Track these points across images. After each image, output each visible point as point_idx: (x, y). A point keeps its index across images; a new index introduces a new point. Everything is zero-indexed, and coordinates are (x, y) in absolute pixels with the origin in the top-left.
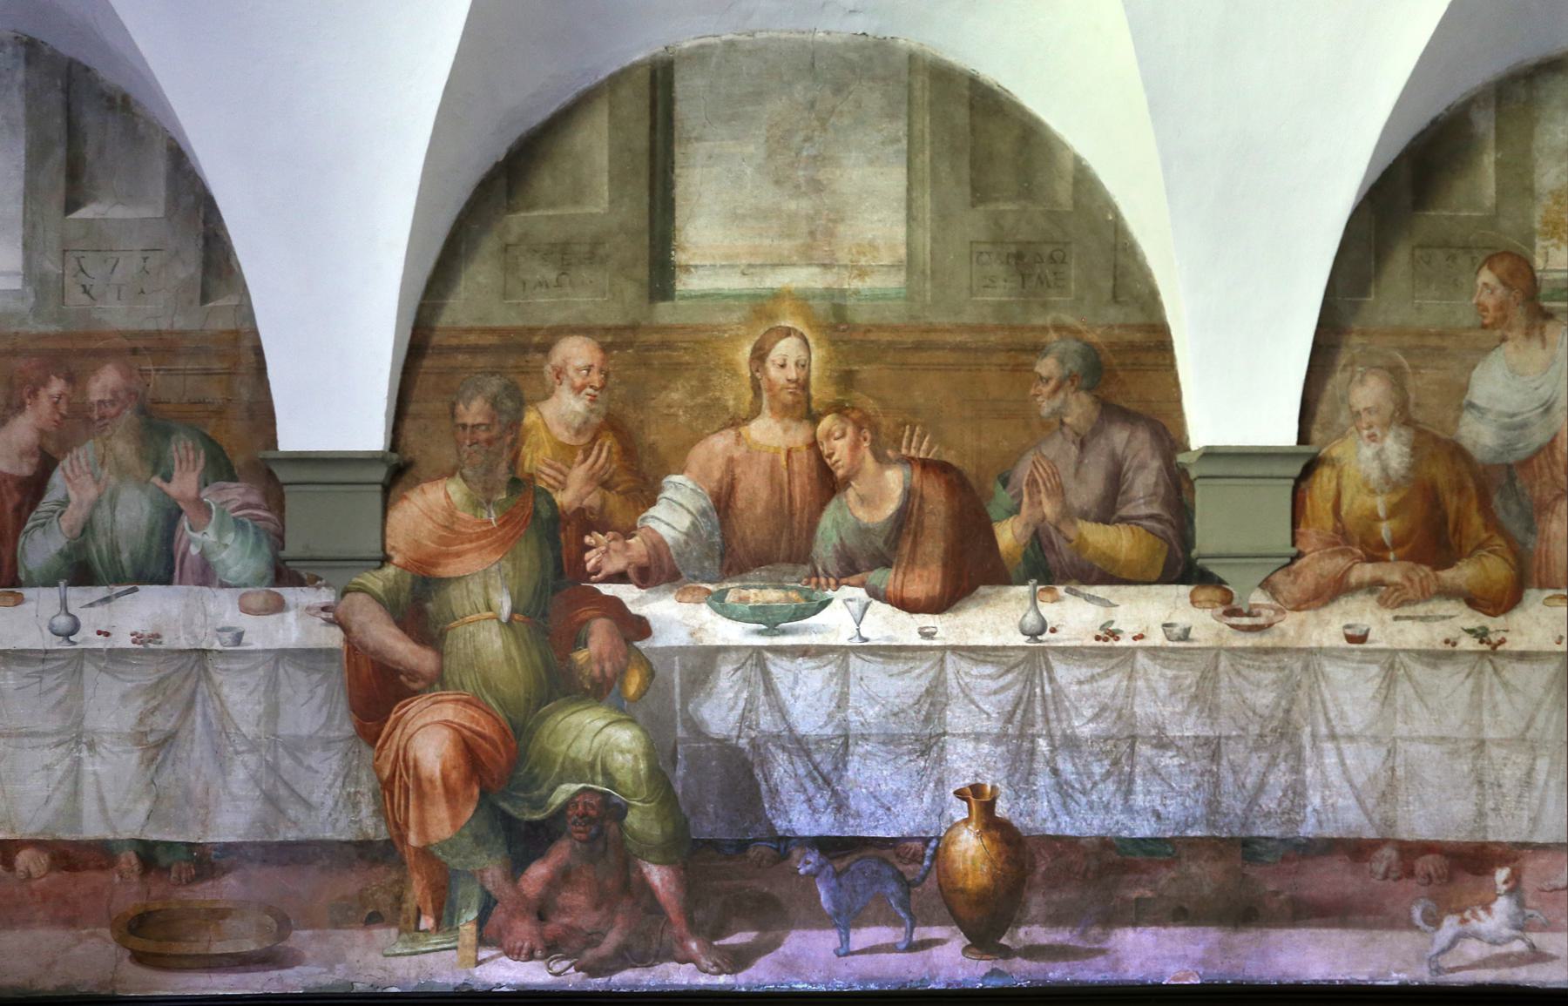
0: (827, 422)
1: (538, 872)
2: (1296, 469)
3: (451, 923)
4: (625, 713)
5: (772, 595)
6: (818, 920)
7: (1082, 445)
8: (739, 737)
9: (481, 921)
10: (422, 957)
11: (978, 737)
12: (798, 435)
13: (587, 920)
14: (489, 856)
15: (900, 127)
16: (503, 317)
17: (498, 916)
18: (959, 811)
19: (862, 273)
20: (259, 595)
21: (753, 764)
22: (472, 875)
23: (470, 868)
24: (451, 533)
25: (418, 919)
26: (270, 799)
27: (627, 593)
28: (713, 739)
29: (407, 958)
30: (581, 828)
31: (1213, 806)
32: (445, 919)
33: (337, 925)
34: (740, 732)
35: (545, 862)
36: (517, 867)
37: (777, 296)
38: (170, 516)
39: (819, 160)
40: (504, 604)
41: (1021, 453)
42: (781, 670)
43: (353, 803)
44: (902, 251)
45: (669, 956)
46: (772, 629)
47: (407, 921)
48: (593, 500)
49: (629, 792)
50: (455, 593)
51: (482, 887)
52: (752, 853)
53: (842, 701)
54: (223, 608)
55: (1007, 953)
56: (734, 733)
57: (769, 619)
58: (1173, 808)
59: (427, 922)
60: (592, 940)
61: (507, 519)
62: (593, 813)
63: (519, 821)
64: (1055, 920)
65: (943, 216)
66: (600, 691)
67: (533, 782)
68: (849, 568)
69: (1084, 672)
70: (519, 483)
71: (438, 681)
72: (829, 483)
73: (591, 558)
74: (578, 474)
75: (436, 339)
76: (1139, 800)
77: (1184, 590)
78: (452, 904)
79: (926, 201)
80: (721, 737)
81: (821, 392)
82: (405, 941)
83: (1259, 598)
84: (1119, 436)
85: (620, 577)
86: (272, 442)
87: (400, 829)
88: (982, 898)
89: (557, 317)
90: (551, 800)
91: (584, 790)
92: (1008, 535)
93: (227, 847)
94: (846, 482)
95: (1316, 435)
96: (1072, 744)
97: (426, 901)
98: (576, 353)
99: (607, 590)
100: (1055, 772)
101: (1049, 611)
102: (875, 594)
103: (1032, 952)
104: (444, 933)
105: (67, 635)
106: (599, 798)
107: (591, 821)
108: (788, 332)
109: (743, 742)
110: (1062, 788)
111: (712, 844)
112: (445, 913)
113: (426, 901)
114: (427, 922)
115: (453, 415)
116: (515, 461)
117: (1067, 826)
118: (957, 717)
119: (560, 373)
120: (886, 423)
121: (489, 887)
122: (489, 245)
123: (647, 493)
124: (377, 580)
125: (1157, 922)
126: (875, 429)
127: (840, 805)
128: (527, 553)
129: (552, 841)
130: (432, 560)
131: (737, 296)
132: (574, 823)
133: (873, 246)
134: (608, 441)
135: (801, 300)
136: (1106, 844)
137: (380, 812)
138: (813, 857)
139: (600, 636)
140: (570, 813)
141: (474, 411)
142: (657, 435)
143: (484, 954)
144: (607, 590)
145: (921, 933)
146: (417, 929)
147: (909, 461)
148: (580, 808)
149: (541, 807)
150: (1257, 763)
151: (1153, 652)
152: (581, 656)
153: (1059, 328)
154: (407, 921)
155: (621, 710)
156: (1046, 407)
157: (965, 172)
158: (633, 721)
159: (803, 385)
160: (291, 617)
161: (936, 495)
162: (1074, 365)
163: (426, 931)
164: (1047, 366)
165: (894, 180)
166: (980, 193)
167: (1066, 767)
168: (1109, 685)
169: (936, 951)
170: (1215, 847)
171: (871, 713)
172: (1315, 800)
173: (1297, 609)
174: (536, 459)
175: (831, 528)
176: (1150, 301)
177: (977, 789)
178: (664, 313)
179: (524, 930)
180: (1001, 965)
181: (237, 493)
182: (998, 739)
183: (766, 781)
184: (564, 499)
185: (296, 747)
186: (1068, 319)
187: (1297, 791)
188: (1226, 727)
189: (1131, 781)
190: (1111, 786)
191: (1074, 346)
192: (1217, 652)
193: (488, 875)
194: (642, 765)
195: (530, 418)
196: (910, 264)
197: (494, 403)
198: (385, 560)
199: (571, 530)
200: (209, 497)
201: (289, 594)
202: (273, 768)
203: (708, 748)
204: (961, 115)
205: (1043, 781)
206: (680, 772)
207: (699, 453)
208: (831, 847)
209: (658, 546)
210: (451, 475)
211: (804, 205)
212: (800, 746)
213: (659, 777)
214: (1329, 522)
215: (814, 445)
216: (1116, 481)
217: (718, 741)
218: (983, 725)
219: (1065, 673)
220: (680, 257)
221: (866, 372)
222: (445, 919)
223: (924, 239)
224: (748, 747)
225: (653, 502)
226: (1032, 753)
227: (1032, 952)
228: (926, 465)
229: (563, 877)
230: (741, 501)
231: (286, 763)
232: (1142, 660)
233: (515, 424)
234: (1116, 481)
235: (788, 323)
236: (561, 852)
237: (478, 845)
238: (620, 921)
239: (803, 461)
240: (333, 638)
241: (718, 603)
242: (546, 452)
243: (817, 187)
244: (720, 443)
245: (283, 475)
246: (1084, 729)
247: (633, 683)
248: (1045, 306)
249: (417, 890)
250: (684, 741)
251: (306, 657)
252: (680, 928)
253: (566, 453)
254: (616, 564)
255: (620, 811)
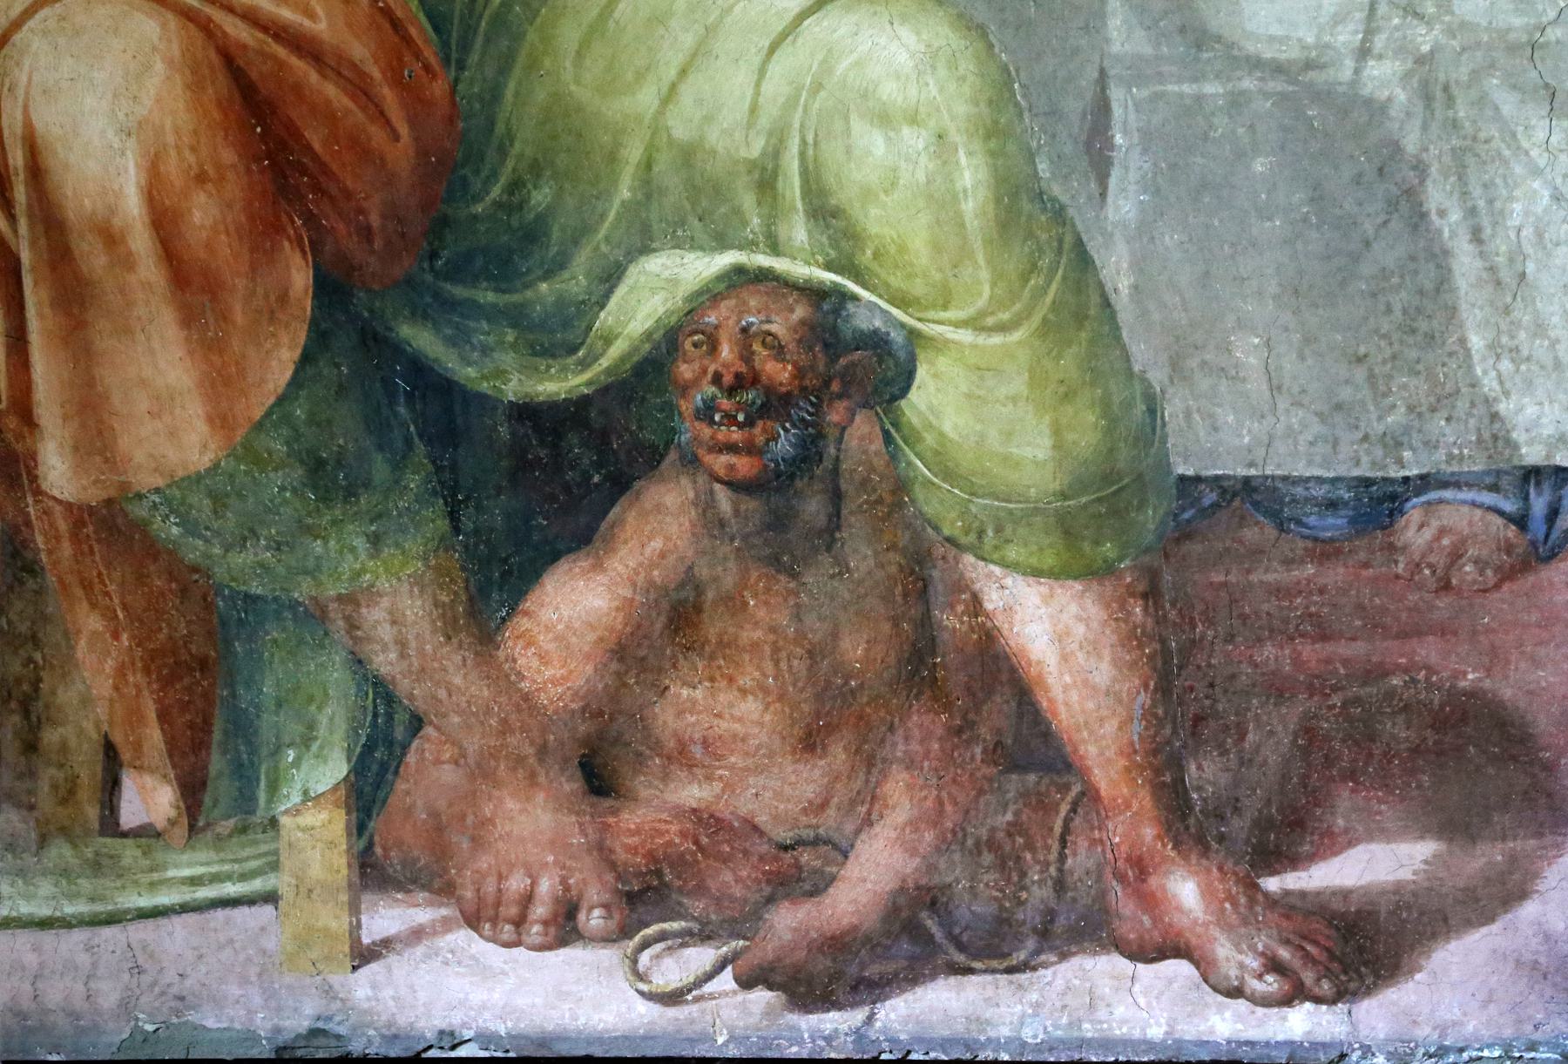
3: (245, 802)
8: (1364, 52)
10: (139, 932)
14: (375, 541)
21: (1421, 168)
22: (314, 616)
23: (303, 590)
25: (112, 786)
28: (1256, 64)
29: (79, 935)
30: (736, 435)
34: (1369, 32)
35: (598, 567)
47: (67, 794)
49: (918, 288)
51: (358, 662)
56: (1347, 37)
62: (779, 373)
63: (484, 402)
78: (243, 727)
80: (1291, 53)
82: (65, 873)
90: (606, 318)
91: (740, 278)
97: (134, 717)
104: (219, 842)
106: (800, 312)
107: (775, 405)
112: (217, 763)
113: (134, 717)
121: (385, 662)
129: (620, 485)
132: (706, 413)
140: (686, 371)
146: (110, 825)
148: (726, 352)
149: (573, 350)
154: (67, 794)
163: (148, 833)
183: (1477, 236)
193: (375, 615)
203: (1237, 101)
206: (1124, 205)
217: (1278, 69)
222: (221, 787)
224: (1401, 96)
237: (325, 498)
250: (1140, 72)
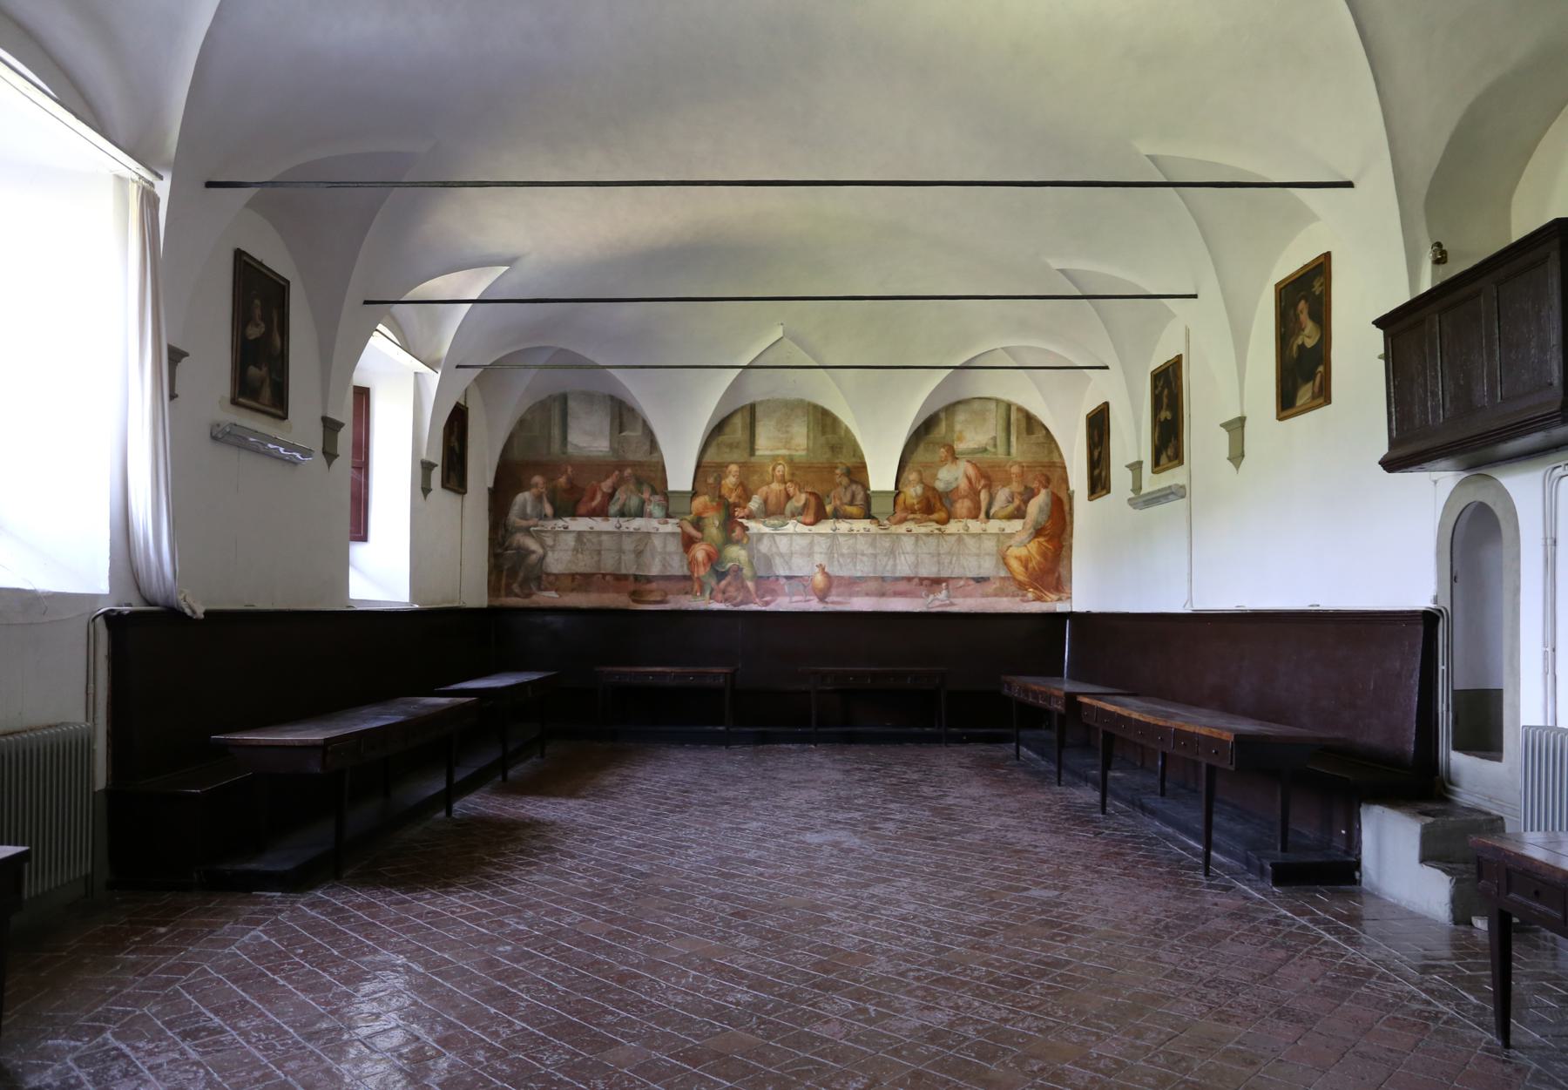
0: (789, 484)
1: (723, 583)
2: (894, 495)
4: (743, 547)
5: (776, 522)
6: (785, 595)
7: (846, 488)
9: (711, 593)
11: (821, 553)
12: (782, 487)
13: (735, 594)
15: (806, 419)
16: (718, 460)
17: (714, 593)
18: (817, 570)
19: (797, 451)
20: (662, 520)
24: (706, 508)
26: (664, 565)
27: (744, 521)
31: (875, 570)
32: (702, 592)
33: (678, 594)
36: (719, 581)
37: (778, 456)
38: (643, 502)
39: (788, 426)
40: (717, 523)
41: (831, 490)
42: (777, 538)
43: (682, 566)
44: (806, 446)
45: (752, 602)
46: (776, 530)
48: (737, 501)
50: (706, 520)
52: (771, 579)
53: (791, 545)
54: (654, 523)
55: (827, 603)
57: (775, 527)
58: (866, 569)
59: (698, 594)
60: (735, 599)
61: (719, 504)
64: (838, 595)
65: (815, 438)
66: (737, 542)
67: (722, 563)
68: (793, 516)
69: (846, 539)
70: (721, 496)
71: (702, 540)
72: (789, 497)
73: (736, 513)
74: (734, 495)
75: (703, 464)
76: (858, 568)
77: (869, 520)
79: (811, 436)
81: (787, 477)
83: (886, 522)
84: (854, 487)
85: (743, 518)
86: (666, 487)
87: (693, 572)
88: (821, 590)
89: (729, 460)
92: (829, 508)
93: (654, 576)
94: (792, 497)
95: (900, 486)
96: (842, 555)
98: (734, 468)
99: (740, 520)
100: (839, 561)
101: (838, 525)
102: (798, 521)
103: (833, 603)
105: (619, 528)
108: (780, 464)
109: (769, 555)
110: (840, 565)
111: (761, 577)
114: (698, 594)
115: (706, 481)
116: (720, 491)
117: (841, 574)
118: (817, 549)
119: (730, 472)
120: (802, 484)
122: (714, 443)
123: (749, 499)
124: (689, 518)
125: (862, 596)
126: (800, 486)
127: (790, 569)
128: (723, 512)
130: (701, 513)
131: (769, 456)
133: (799, 445)
134: (741, 488)
135: (783, 457)
136: (850, 578)
137: (689, 569)
138: (784, 580)
139: (738, 530)
141: (711, 480)
142: (751, 487)
143: (711, 601)
144: (740, 520)
145: (808, 598)
147: (807, 492)
150: (885, 559)
151: (862, 534)
152: (734, 535)
153: (841, 463)
155: (742, 546)
156: (838, 480)
157: (820, 428)
158: (744, 549)
159: (783, 476)
160: (669, 525)
161: (813, 500)
162: (844, 471)
164: (838, 471)
165: (804, 430)
166: (824, 432)
167: (841, 560)
168: (851, 541)
169: (812, 602)
170: (876, 578)
171: (797, 548)
172: (899, 568)
173: (895, 524)
174: (725, 491)
175: (790, 507)
176: (862, 457)
177: (821, 565)
178: (753, 459)
179: (720, 596)
180: (826, 606)
181: (657, 498)
182: (826, 554)
184: (731, 500)
185: (670, 554)
186: (843, 461)
187: (895, 565)
188: (878, 551)
189: (856, 563)
190: (851, 565)
191: (844, 467)
192: (876, 534)
194: (747, 559)
195: (723, 482)
196: (808, 449)
197: (715, 479)
198: (691, 513)
199: (732, 507)
200: (652, 498)
201: (669, 520)
202: (664, 559)
204: (820, 416)
205: (836, 563)
207: (760, 490)
208: (788, 578)
209: (751, 511)
210: (705, 494)
211: (784, 436)
212: (781, 555)
213: (751, 562)
214: (903, 505)
215: (785, 489)
216: (853, 497)
218: (822, 550)
219: (841, 539)
220: (756, 447)
221: (797, 473)
223: (811, 445)
225: (749, 501)
226: (833, 557)
227: (833, 603)
228: (810, 493)
229: (729, 584)
230: (769, 501)
231: (668, 557)
232: (858, 536)
233: (720, 483)
234: (853, 497)
235: (781, 462)
236: (729, 578)
238: (741, 594)
239: (783, 493)
240: (679, 530)
241: (764, 523)
242: (727, 490)
243: (787, 432)
244: (765, 488)
245: (669, 495)
246: (845, 551)
247: (745, 541)
248: (838, 458)
249: (696, 587)
251: (673, 534)
252: (755, 596)
253: (731, 490)
254: (741, 515)
255: (741, 570)
